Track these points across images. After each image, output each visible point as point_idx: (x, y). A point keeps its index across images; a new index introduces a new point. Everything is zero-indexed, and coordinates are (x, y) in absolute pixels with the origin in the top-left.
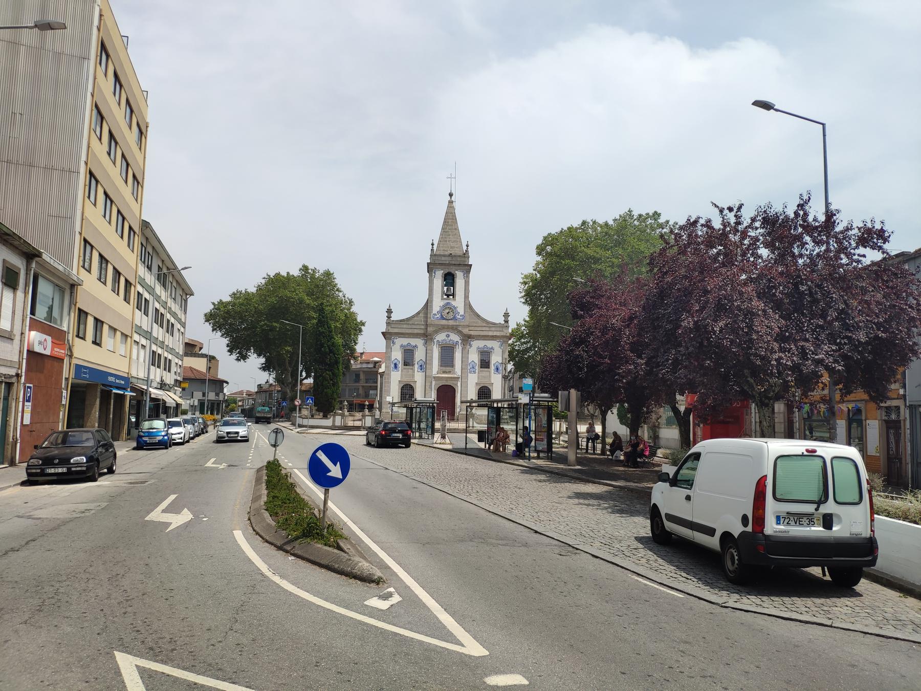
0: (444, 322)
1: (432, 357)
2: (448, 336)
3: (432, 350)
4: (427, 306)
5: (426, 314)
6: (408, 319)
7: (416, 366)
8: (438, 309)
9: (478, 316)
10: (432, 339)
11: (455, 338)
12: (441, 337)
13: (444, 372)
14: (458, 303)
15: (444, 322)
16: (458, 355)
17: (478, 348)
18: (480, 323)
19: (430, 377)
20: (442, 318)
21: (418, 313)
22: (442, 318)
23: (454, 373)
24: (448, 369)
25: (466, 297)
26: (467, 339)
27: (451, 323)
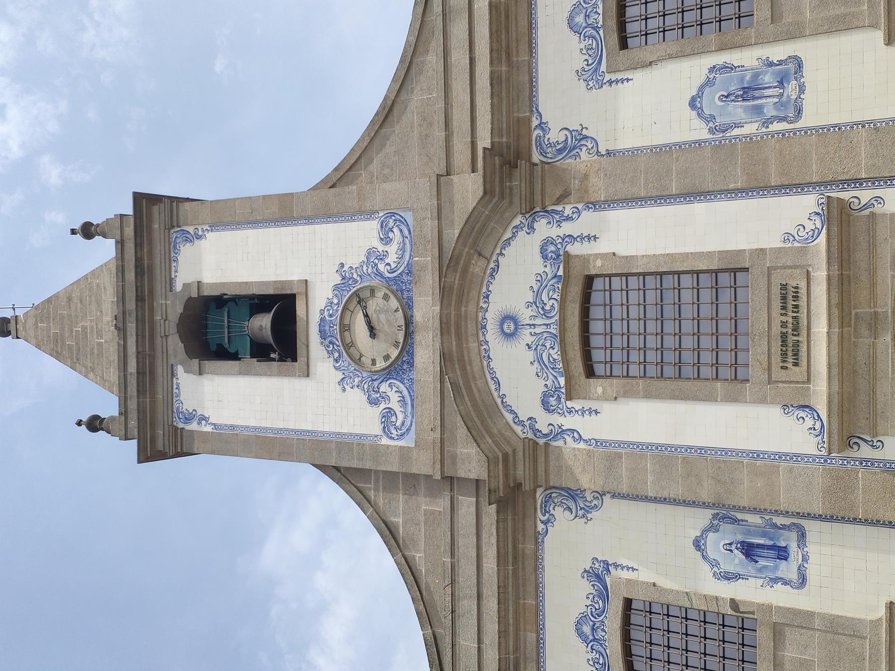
0: (426, 355)
1: (665, 455)
2: (510, 325)
3: (611, 453)
4: (352, 471)
5: (391, 480)
6: (427, 615)
7: (752, 591)
8: (356, 397)
9: (387, 114)
10: (539, 449)
11: (518, 275)
12: (518, 376)
13: (791, 348)
14: (311, 260)
15: (426, 355)
16: (631, 235)
17: (592, 76)
18: (424, 94)
19: (839, 484)
20: (400, 367)
21: (390, 534)
22: (400, 367)
23: (794, 255)
24: (760, 316)
25: (283, 211)
26: (520, 173)
27: (426, 308)
